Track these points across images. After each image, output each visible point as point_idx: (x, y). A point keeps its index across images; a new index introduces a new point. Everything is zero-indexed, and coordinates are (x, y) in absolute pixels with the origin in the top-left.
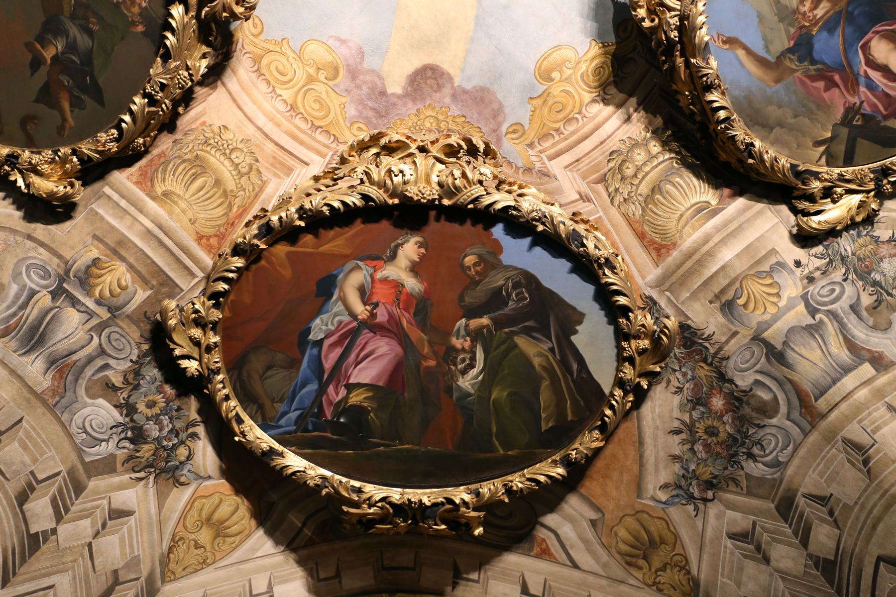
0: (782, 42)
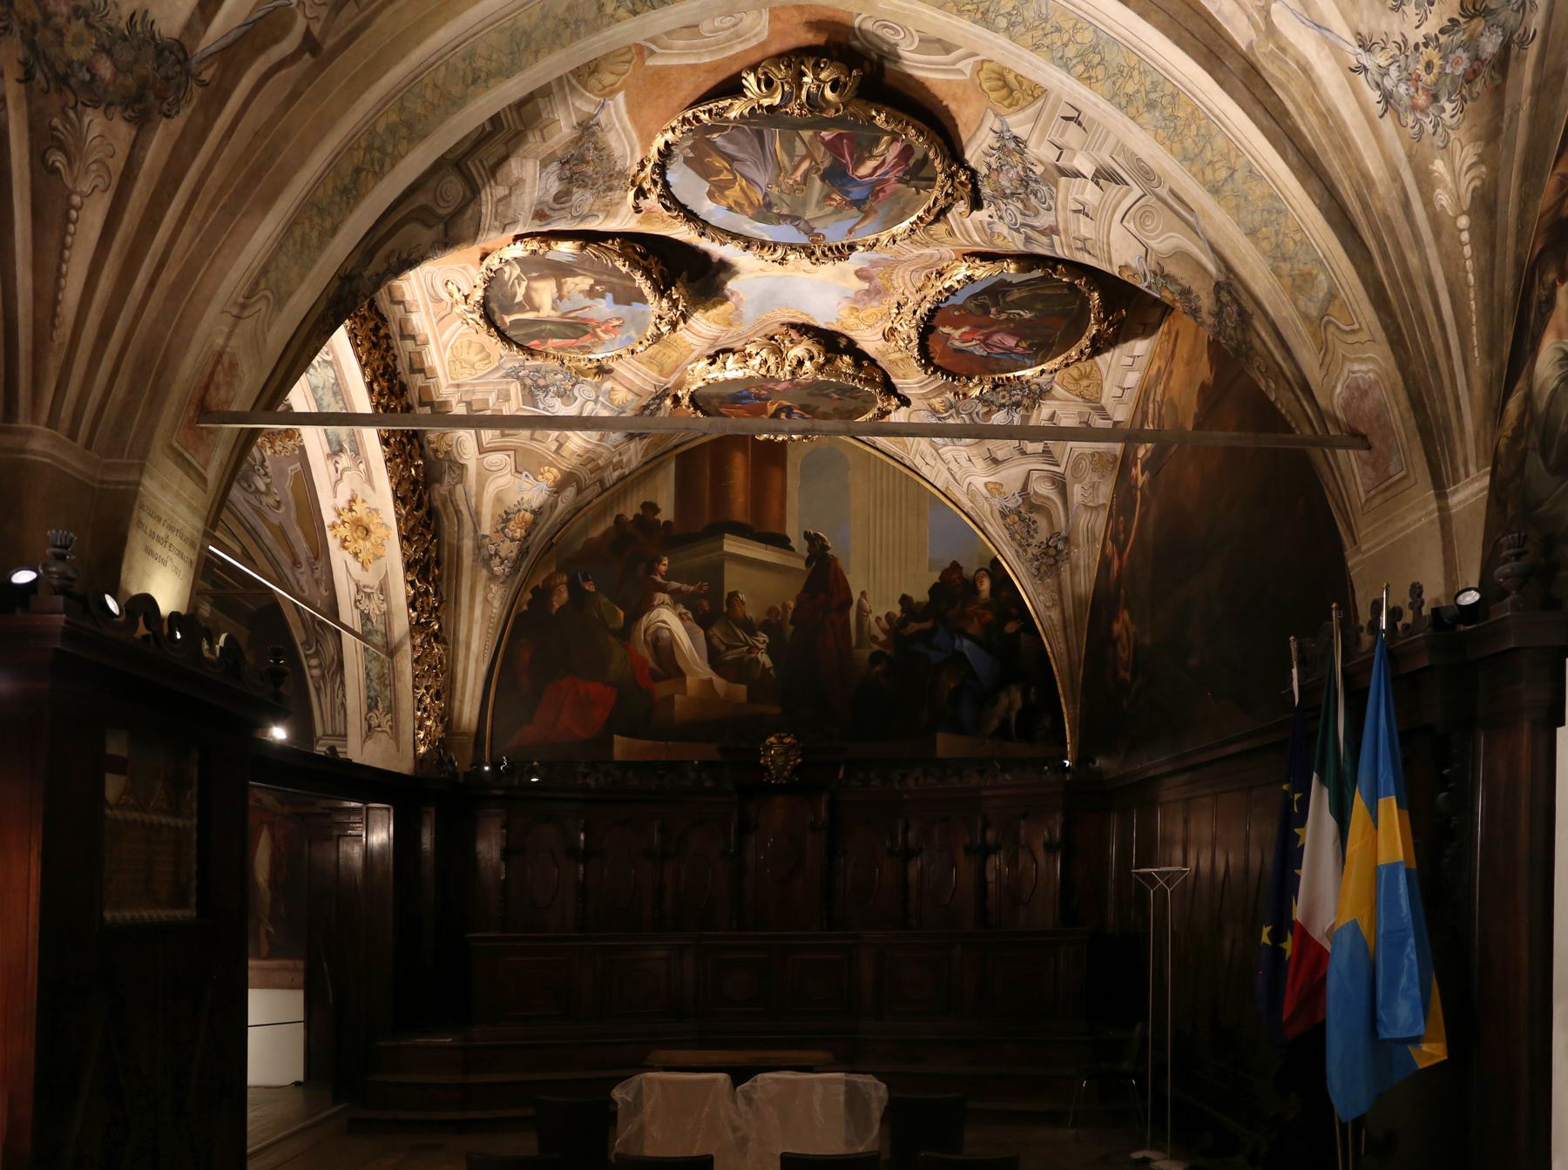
0: (855, 211)
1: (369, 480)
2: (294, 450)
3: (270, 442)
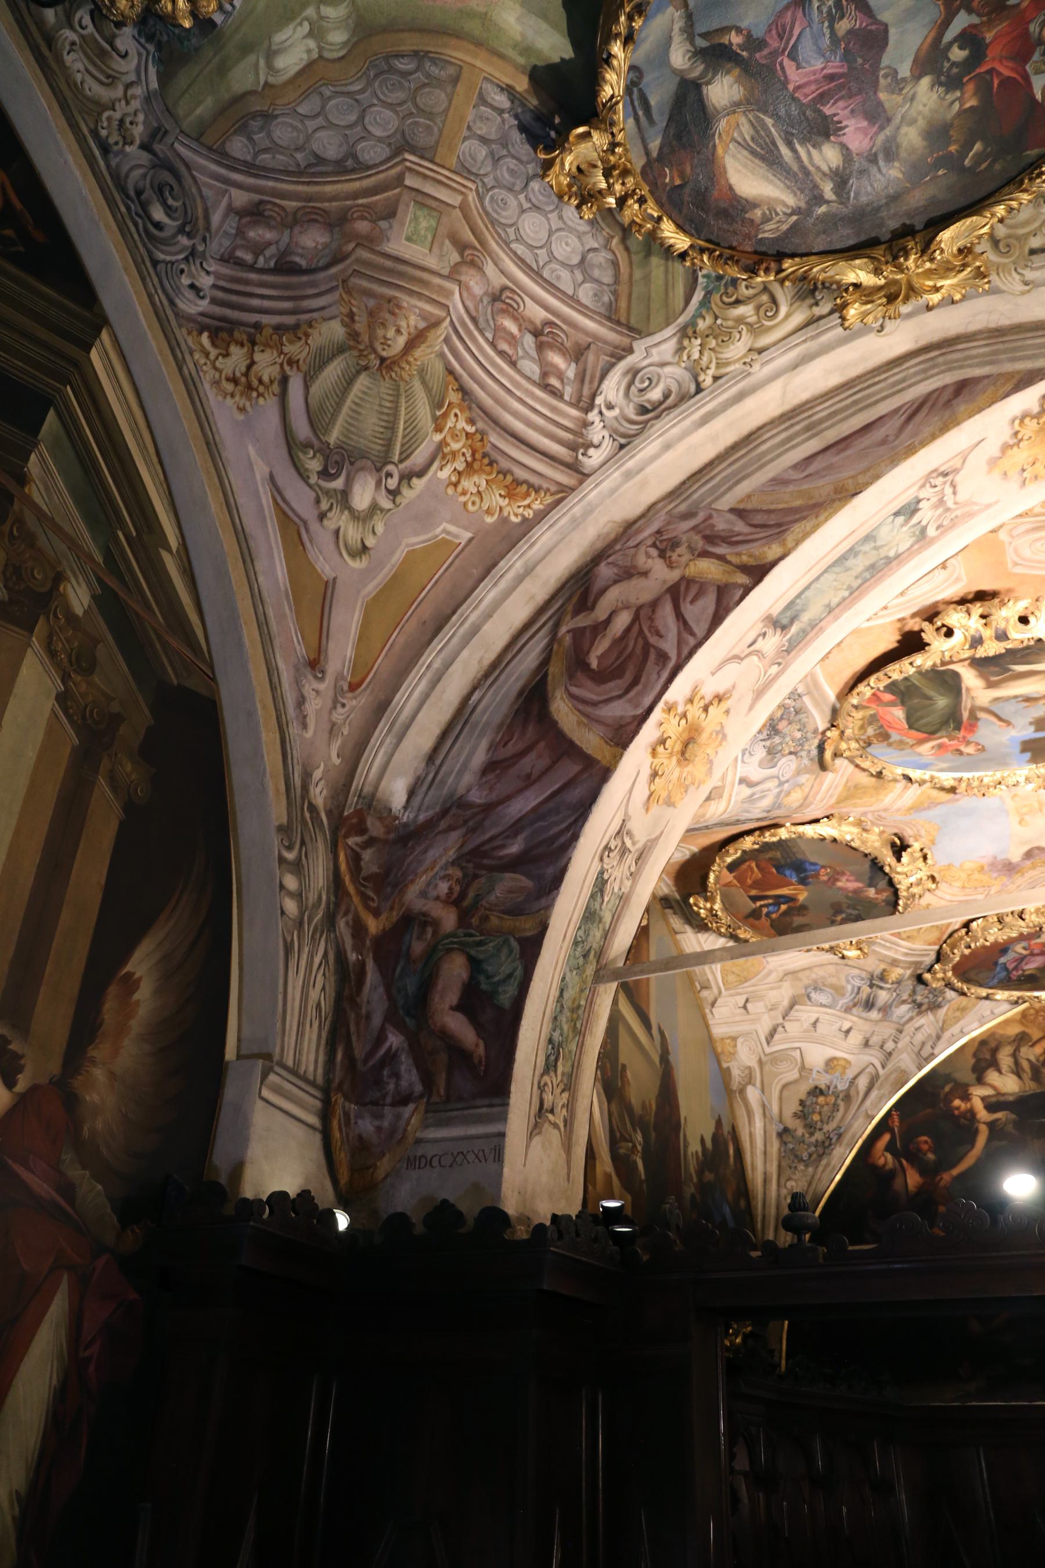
1: (759, 694)
2: (488, 512)
3: (469, 465)
